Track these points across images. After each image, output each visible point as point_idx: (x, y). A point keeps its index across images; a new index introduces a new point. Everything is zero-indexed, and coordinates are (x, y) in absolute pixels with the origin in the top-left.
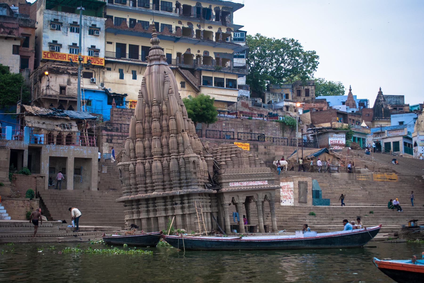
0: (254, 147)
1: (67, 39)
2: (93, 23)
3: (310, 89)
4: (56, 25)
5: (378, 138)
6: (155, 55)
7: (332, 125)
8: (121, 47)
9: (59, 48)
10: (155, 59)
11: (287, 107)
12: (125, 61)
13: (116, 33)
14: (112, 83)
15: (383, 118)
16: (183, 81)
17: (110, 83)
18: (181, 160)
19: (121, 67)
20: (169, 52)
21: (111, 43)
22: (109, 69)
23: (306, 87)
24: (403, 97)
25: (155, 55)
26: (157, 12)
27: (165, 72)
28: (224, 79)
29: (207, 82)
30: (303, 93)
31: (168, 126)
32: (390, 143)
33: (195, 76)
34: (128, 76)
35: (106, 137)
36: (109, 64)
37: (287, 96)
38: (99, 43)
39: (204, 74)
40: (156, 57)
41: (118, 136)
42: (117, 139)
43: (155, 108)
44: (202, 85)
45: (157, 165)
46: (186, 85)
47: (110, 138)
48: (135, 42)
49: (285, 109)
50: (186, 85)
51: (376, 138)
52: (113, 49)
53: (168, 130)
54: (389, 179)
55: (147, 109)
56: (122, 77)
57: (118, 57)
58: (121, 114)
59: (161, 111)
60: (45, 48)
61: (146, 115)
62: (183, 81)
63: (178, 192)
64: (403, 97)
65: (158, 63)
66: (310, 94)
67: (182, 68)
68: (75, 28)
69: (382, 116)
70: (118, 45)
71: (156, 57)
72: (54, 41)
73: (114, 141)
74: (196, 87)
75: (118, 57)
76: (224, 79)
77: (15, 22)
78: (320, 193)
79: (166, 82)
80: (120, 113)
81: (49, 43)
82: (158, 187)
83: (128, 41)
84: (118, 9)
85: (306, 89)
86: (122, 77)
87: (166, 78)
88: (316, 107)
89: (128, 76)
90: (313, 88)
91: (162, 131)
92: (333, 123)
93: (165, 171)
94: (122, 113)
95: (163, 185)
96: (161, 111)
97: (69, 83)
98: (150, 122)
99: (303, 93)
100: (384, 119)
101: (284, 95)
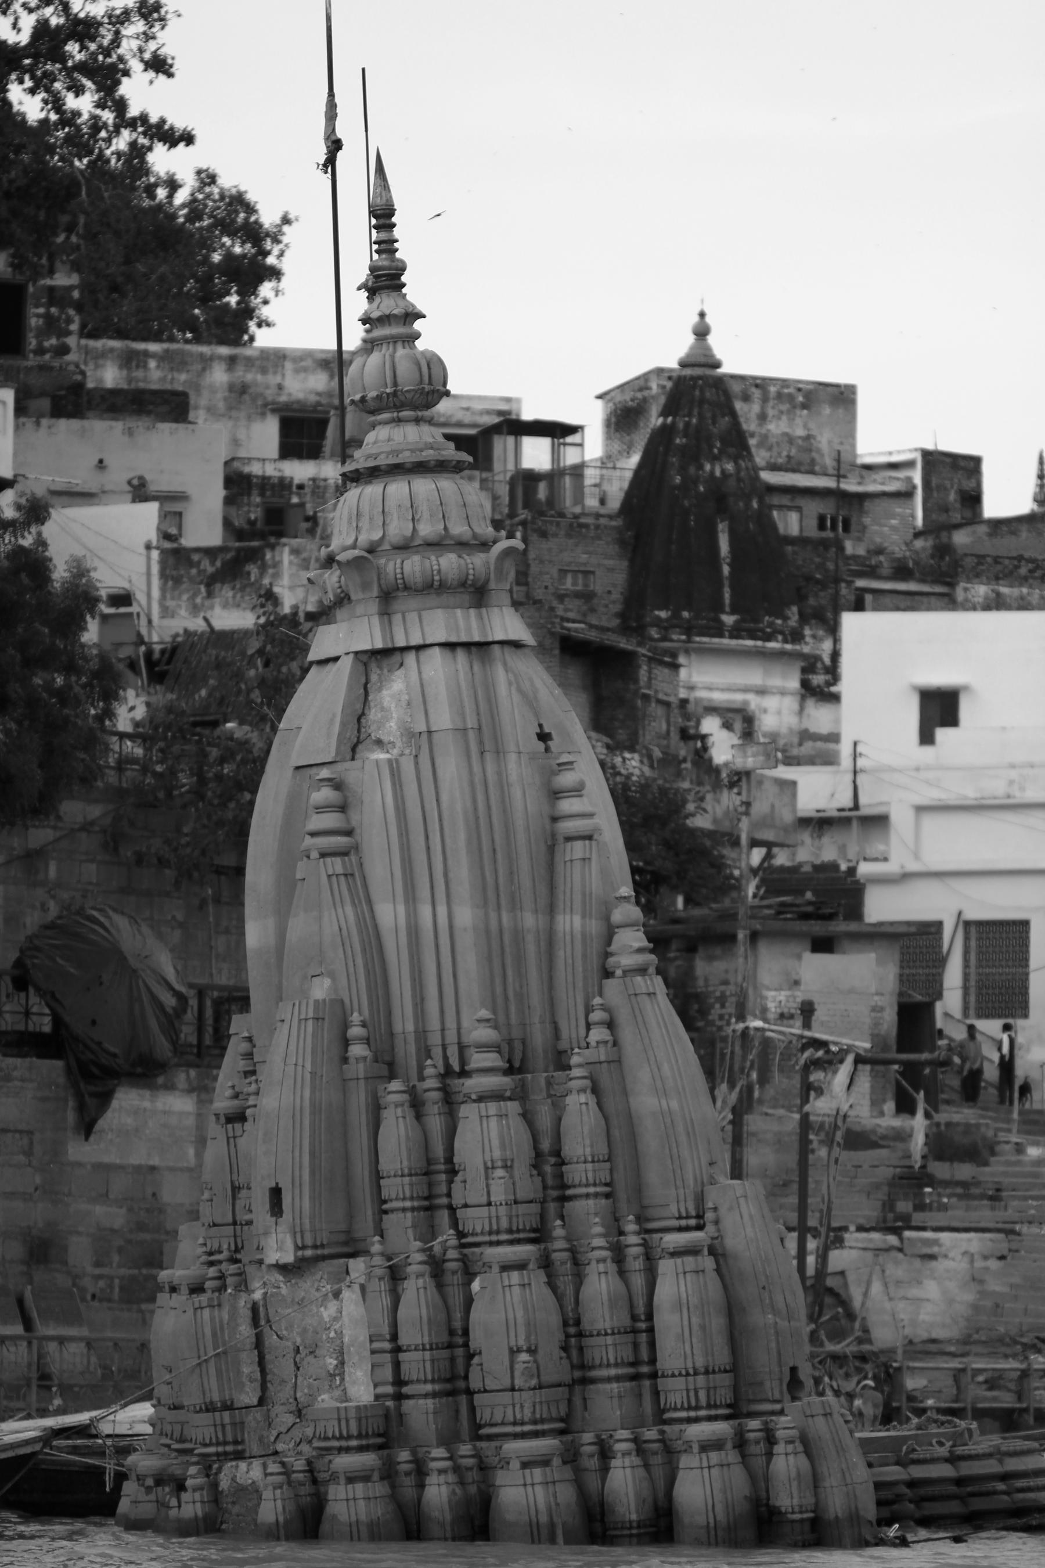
6: (435, 545)
10: (434, 588)
15: (729, 619)
24: (842, 398)
25: (435, 545)
27: (544, 737)
31: (641, 1324)
32: (931, 930)
40: (449, 563)
43: (486, 1136)
53: (643, 1370)
55: (396, 1131)
59: (548, 1159)
61: (391, 1187)
64: (842, 398)
65: (467, 625)
69: (718, 607)
71: (449, 563)
79: (578, 849)
87: (567, 805)
91: (581, 1378)
96: (548, 1159)
98: (453, 1275)
100: (736, 632)
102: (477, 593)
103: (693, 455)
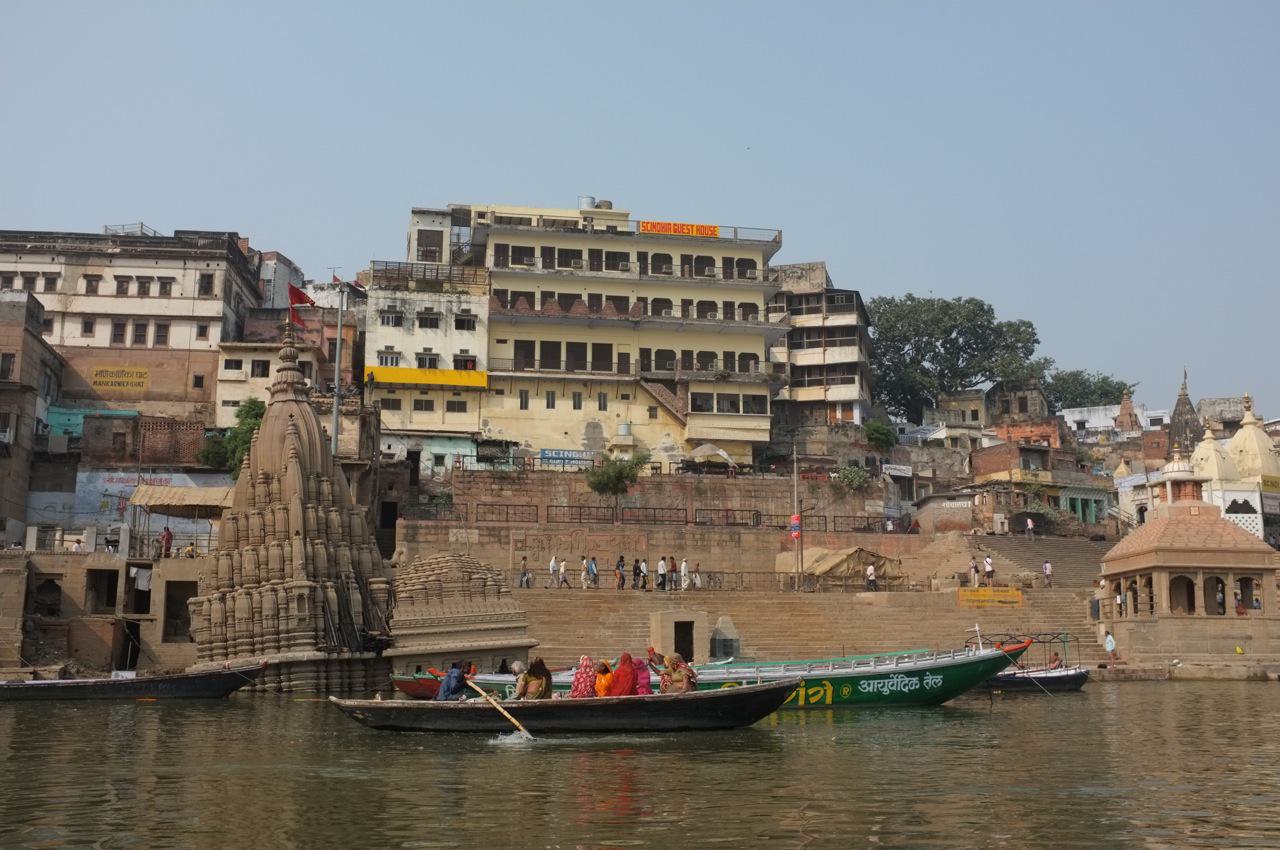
0: (731, 536)
1: (412, 341)
2: (464, 306)
3: (1029, 398)
4: (394, 317)
5: (1143, 497)
7: (1010, 475)
8: (524, 350)
9: (397, 359)
11: (955, 440)
12: (533, 375)
13: (514, 322)
14: (506, 418)
16: (654, 404)
17: (499, 418)
18: (282, 594)
19: (524, 387)
20: (624, 350)
21: (505, 342)
22: (500, 392)
23: (1020, 394)
26: (594, 274)
28: (738, 395)
29: (701, 405)
30: (1015, 407)
33: (675, 394)
34: (537, 404)
35: (404, 531)
36: (495, 387)
37: (975, 415)
38: (475, 343)
39: (695, 389)
41: (427, 527)
42: (426, 534)
44: (690, 410)
45: (242, 603)
46: (660, 413)
47: (410, 531)
48: (551, 337)
49: (948, 443)
50: (660, 413)
51: (1139, 497)
52: (508, 352)
54: (1000, 602)
56: (524, 406)
57: (517, 367)
58: (470, 482)
60: (371, 362)
62: (654, 404)
63: (273, 657)
66: (1030, 408)
67: (647, 380)
68: (429, 320)
70: (519, 345)
72: (387, 347)
73: (421, 538)
74: (679, 415)
75: (517, 367)
76: (738, 395)
77: (316, 319)
78: (735, 644)
80: (467, 479)
81: (379, 352)
82: (244, 647)
83: (538, 336)
84: (514, 276)
85: (1020, 398)
86: (524, 406)
88: (1036, 435)
89: (537, 404)
90: (1035, 393)
92: (1013, 472)
93: (254, 613)
94: (471, 479)
95: (226, 648)
97: (339, 429)
99: (1015, 407)
101: (968, 413)
102: (284, 391)
103: (1180, 414)
